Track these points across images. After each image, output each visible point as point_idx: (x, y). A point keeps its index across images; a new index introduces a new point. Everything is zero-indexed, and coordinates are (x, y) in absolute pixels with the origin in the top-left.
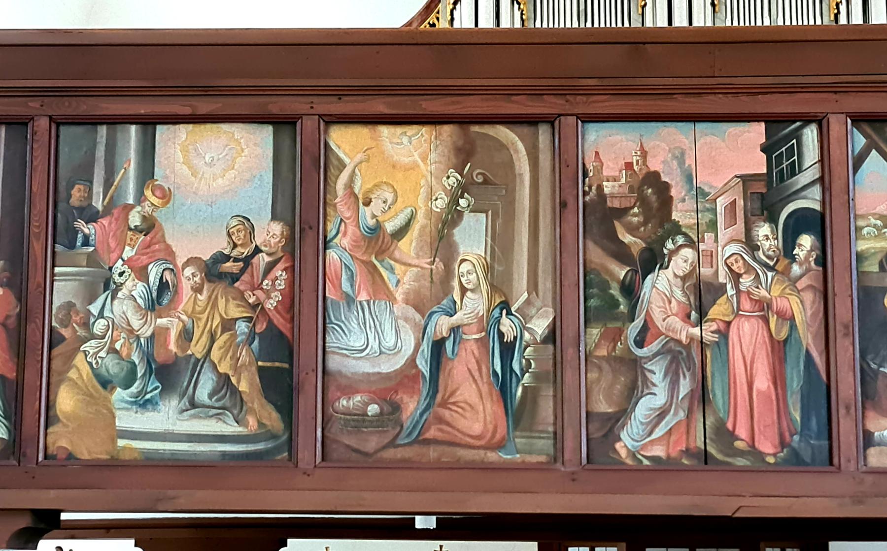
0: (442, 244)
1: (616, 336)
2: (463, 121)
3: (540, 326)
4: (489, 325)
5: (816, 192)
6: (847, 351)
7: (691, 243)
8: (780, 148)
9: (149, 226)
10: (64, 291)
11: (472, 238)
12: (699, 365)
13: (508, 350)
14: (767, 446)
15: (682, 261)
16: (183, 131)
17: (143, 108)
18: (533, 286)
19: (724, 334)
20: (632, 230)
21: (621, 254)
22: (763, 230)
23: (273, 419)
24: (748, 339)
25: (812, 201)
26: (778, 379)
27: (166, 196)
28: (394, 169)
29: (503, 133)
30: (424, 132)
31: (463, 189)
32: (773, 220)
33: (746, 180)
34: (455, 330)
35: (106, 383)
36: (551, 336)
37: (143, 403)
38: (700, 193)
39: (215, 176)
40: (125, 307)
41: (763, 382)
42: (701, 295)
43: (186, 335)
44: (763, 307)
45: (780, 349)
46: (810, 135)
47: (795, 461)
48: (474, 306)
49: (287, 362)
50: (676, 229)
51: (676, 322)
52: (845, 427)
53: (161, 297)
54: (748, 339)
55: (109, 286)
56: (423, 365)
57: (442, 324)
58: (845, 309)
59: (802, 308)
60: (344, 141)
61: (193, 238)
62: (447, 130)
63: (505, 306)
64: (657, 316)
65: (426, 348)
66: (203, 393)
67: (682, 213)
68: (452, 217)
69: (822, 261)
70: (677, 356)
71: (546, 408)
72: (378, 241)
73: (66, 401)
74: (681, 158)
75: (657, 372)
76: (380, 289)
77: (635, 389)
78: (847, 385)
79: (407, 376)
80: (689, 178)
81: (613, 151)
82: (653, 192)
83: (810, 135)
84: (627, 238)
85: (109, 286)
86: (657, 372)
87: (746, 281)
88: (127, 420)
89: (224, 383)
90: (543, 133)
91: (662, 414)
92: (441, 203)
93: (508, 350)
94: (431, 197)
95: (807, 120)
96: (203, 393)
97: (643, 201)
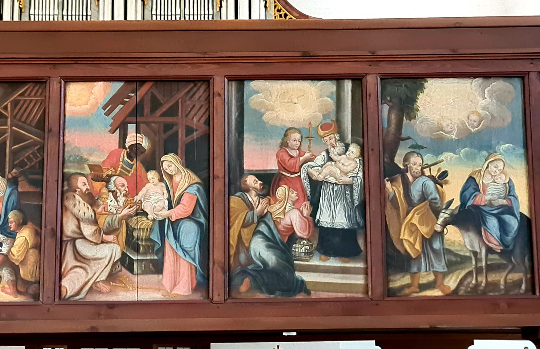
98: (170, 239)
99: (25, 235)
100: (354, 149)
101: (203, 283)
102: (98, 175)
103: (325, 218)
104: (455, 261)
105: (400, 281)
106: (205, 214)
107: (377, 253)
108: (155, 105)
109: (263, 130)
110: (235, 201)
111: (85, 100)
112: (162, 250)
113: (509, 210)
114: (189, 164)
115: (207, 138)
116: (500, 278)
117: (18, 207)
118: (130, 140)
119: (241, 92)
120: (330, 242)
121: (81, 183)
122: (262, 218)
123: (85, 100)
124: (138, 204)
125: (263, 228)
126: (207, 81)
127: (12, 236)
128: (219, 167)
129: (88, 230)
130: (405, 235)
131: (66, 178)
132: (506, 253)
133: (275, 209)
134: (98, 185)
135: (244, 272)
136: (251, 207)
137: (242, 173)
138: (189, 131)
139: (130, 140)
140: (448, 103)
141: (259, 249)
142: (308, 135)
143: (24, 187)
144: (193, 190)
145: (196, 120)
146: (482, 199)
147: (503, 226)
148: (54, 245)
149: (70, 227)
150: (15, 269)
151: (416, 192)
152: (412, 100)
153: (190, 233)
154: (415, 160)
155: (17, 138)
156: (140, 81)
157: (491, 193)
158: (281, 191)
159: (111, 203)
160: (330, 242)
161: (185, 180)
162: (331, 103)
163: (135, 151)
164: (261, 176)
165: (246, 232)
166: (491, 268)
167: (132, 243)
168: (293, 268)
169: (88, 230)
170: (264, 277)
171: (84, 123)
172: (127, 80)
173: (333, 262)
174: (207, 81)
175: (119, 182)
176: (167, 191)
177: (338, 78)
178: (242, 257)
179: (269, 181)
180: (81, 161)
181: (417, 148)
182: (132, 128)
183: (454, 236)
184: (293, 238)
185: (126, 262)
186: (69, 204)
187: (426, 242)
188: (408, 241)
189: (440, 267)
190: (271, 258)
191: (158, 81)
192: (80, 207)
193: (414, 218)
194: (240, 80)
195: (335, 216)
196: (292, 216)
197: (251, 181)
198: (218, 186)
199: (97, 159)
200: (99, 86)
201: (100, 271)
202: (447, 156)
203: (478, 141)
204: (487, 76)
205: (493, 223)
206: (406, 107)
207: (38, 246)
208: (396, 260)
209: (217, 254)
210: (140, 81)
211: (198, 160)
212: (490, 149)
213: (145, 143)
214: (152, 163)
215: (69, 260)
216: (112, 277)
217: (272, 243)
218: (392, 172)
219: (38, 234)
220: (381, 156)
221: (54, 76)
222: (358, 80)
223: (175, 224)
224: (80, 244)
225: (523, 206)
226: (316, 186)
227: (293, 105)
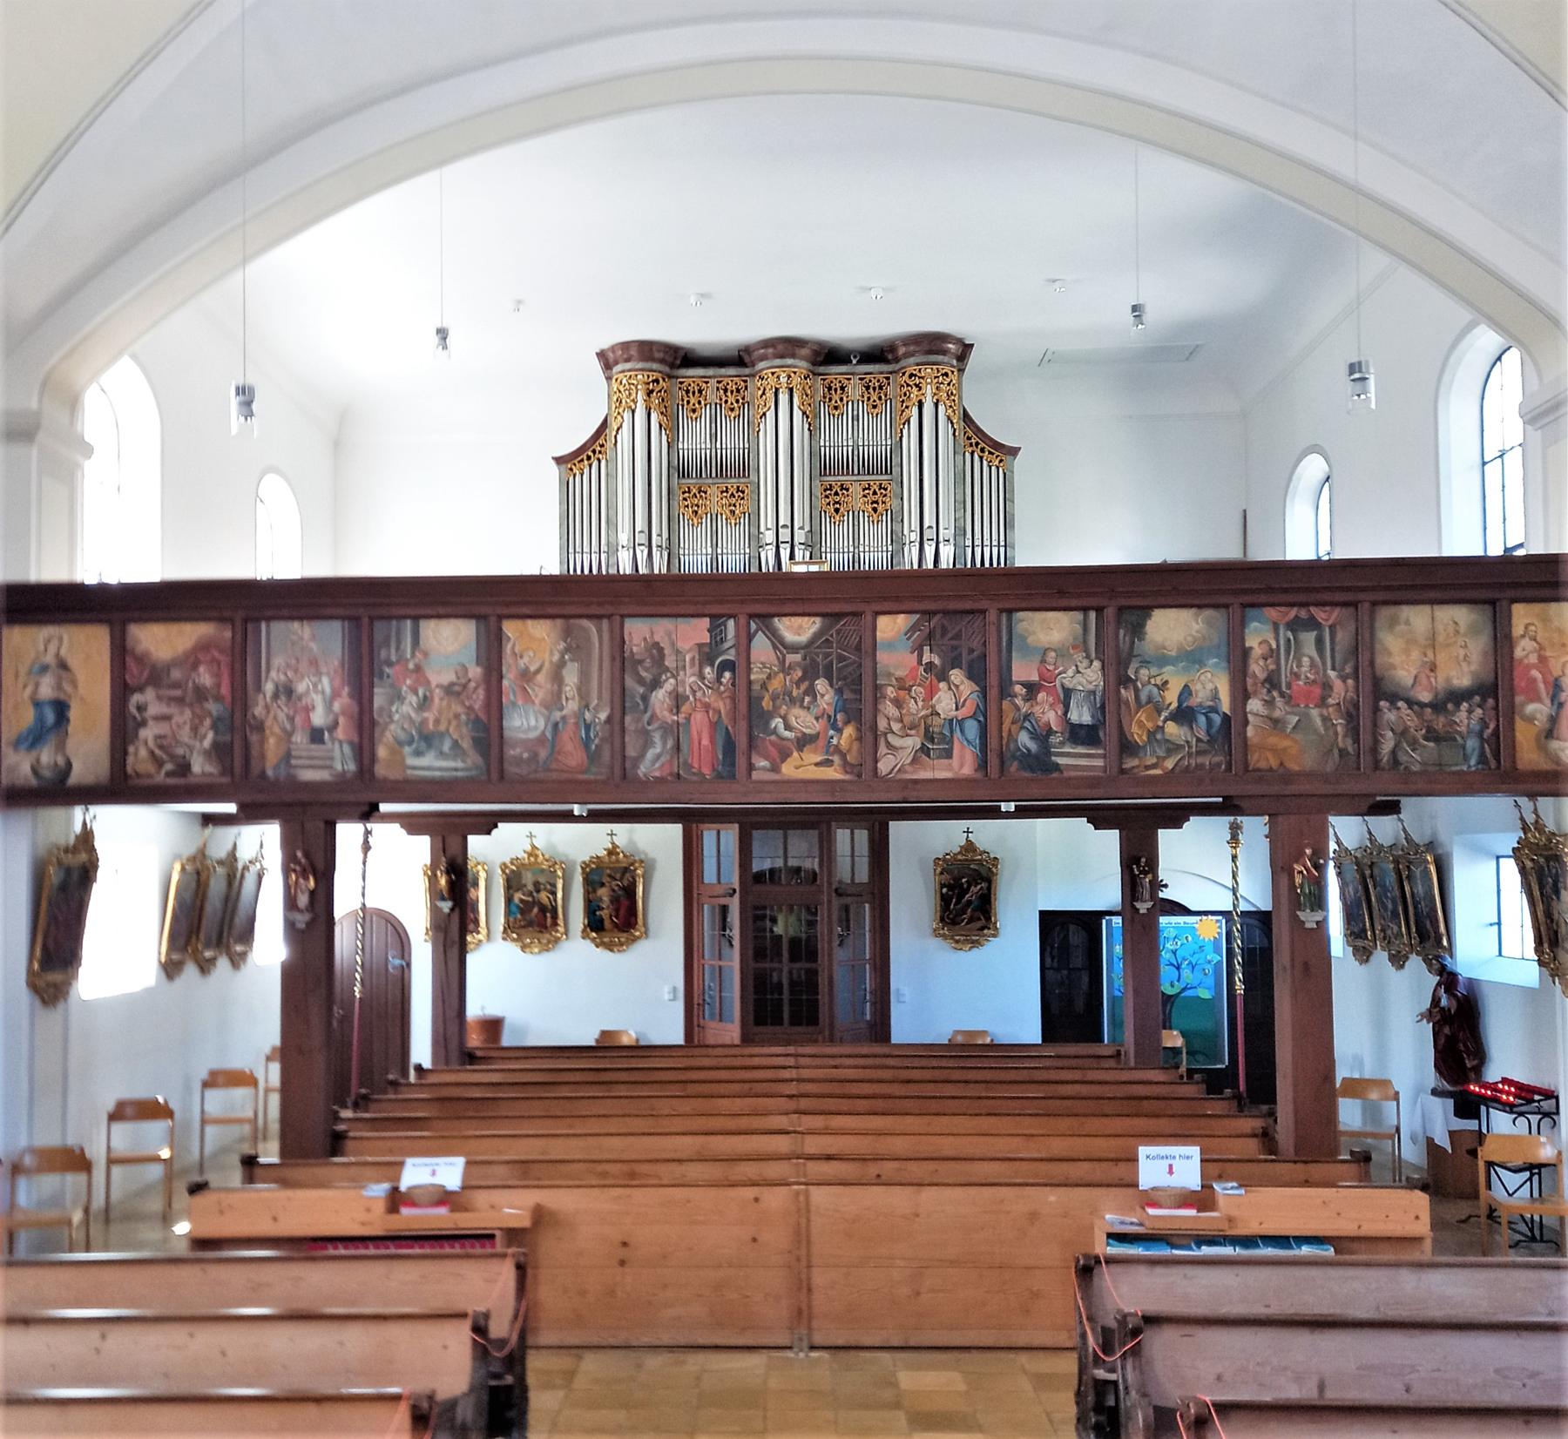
0: (557, 678)
1: (639, 720)
3: (603, 716)
4: (579, 715)
5: (733, 651)
7: (674, 676)
8: (716, 630)
11: (571, 677)
12: (675, 733)
13: (588, 728)
18: (600, 698)
19: (688, 719)
20: (647, 670)
21: (641, 681)
22: (708, 670)
24: (699, 719)
25: (730, 656)
26: (712, 741)
29: (585, 623)
31: (567, 650)
32: (712, 665)
33: (700, 646)
34: (564, 718)
36: (609, 720)
38: (678, 652)
41: (705, 742)
42: (678, 700)
44: (707, 706)
45: (714, 726)
46: (731, 623)
48: (572, 706)
50: (667, 669)
51: (666, 713)
56: (549, 735)
57: (557, 715)
58: (743, 707)
59: (723, 706)
62: (559, 622)
63: (587, 706)
64: (658, 711)
65: (550, 728)
67: (669, 662)
68: (561, 664)
69: (733, 685)
74: (669, 634)
77: (647, 744)
78: (742, 742)
80: (673, 644)
81: (638, 632)
84: (644, 674)
87: (699, 694)
90: (605, 623)
91: (658, 757)
92: (556, 657)
93: (588, 728)
94: (552, 654)
95: (730, 616)
97: (652, 657)
98: (958, 734)
99: (849, 731)
102: (903, 686)
106: (981, 715)
108: (944, 631)
109: (1027, 650)
110: (1006, 704)
112: (951, 742)
114: (971, 676)
117: (844, 710)
118: (925, 659)
119: (1010, 620)
121: (890, 692)
122: (1027, 717)
123: (891, 627)
124: (933, 707)
125: (1027, 724)
126: (983, 612)
127: (840, 731)
128: (993, 679)
129: (896, 727)
134: (902, 693)
135: (1014, 757)
136: (1018, 709)
138: (971, 651)
139: (925, 659)
143: (847, 695)
144: (974, 696)
145: (975, 643)
149: (882, 724)
153: (972, 728)
156: (935, 613)
161: (967, 688)
163: (930, 667)
165: (1014, 728)
167: (929, 736)
169: (896, 727)
171: (890, 645)
172: (923, 612)
174: (983, 612)
175: (918, 690)
176: (954, 697)
178: (1012, 746)
180: (889, 675)
182: (927, 649)
185: (924, 750)
186: (880, 707)
192: (890, 709)
194: (1010, 611)
197: (1018, 689)
198: (993, 693)
199: (900, 673)
207: (860, 739)
209: (993, 742)
210: (935, 613)
211: (977, 674)
213: (937, 661)
214: (943, 676)
216: (915, 761)
219: (859, 730)
221: (868, 609)
223: (961, 722)
224: (890, 737)
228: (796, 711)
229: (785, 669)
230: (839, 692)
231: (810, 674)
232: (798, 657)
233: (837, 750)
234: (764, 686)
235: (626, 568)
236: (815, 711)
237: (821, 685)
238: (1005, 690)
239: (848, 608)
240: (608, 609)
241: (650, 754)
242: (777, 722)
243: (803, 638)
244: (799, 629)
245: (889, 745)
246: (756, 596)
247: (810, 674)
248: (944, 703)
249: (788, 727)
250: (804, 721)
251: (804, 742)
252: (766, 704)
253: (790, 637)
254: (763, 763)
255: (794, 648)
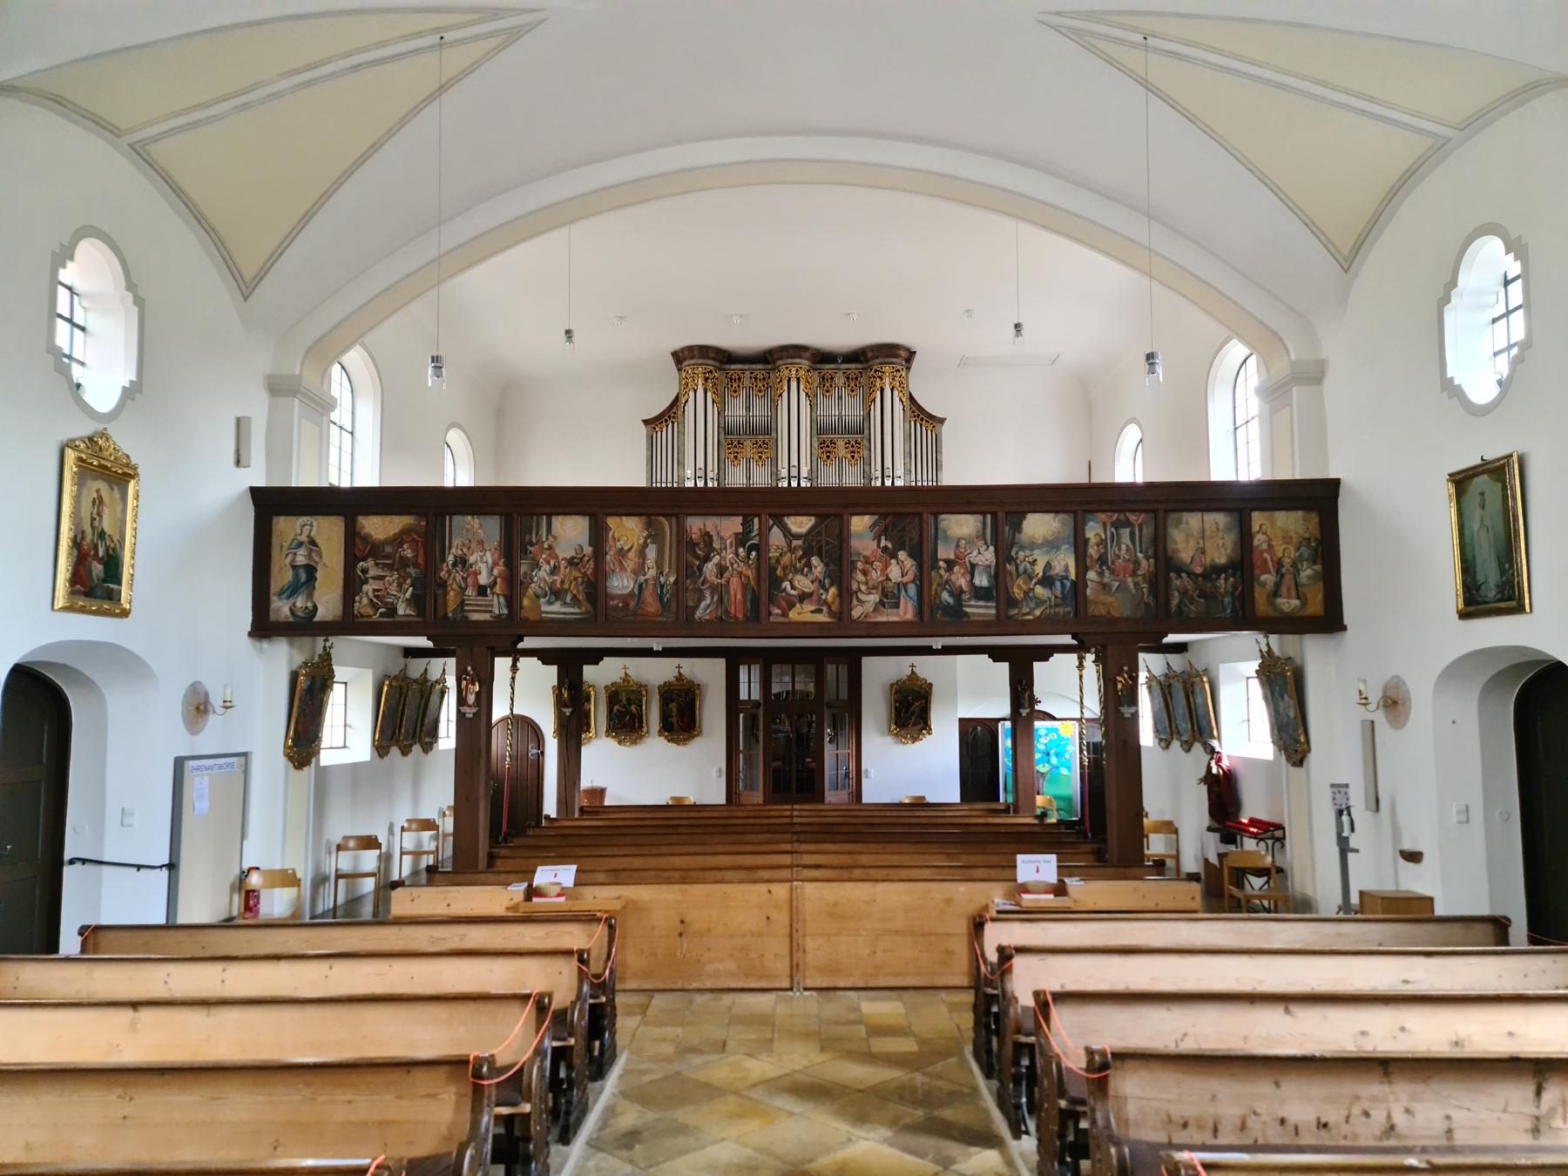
0: (642, 554)
1: (695, 583)
2: (649, 515)
3: (672, 579)
4: (656, 579)
6: (765, 586)
8: (747, 524)
9: (550, 547)
10: (523, 569)
11: (651, 553)
12: (720, 591)
13: (662, 587)
14: (740, 616)
15: (716, 559)
16: (560, 518)
17: (547, 510)
21: (697, 557)
23: (590, 608)
24: (735, 582)
25: (755, 541)
26: (744, 596)
27: (555, 538)
28: (627, 530)
29: (662, 519)
30: (637, 519)
33: (736, 534)
35: (538, 597)
36: (676, 582)
37: (550, 603)
39: (571, 532)
40: (543, 573)
41: (739, 597)
42: (721, 570)
43: (562, 582)
44: (740, 574)
45: (745, 587)
46: (756, 520)
47: (748, 620)
48: (652, 573)
49: (595, 587)
52: (763, 610)
53: (554, 570)
54: (735, 582)
55: (538, 567)
57: (642, 579)
58: (764, 574)
60: (612, 522)
61: (565, 552)
66: (568, 600)
67: (716, 545)
68: (645, 545)
70: (714, 589)
71: (674, 603)
72: (622, 553)
73: (526, 602)
75: (708, 594)
76: (623, 568)
77: (701, 598)
79: (632, 594)
81: (695, 525)
82: (707, 538)
83: (756, 520)
85: (538, 567)
86: (708, 594)
88: (544, 608)
89: (574, 597)
93: (662, 587)
96: (568, 600)
99: (833, 590)
100: (992, 548)
101: (920, 612)
102: (867, 561)
103: (977, 582)
104: (1040, 602)
105: (1014, 612)
106: (921, 579)
107: (1003, 598)
109: (946, 538)
111: (860, 524)
113: (1066, 578)
115: (921, 542)
116: (1061, 610)
120: (979, 593)
121: (860, 565)
122: (947, 582)
123: (860, 524)
127: (827, 591)
129: (863, 588)
130: (1016, 590)
131: (853, 562)
132: (1064, 598)
133: (953, 577)
137: (937, 560)
139: (883, 543)
140: (1038, 525)
141: (945, 596)
142: (969, 541)
145: (915, 534)
146: (1053, 573)
147: (1063, 585)
148: (847, 595)
149: (855, 586)
150: (829, 607)
151: (1021, 568)
152: (1020, 524)
153: (912, 589)
154: (1021, 554)
155: (828, 543)
157: (1058, 569)
158: (956, 569)
159: (874, 575)
160: (979, 593)
161: (909, 563)
162: (980, 525)
163: (885, 549)
164: (946, 561)
166: (1057, 605)
167: (885, 594)
168: (962, 606)
170: (946, 608)
171: (860, 535)
173: (981, 603)
174: (920, 515)
175: (877, 564)
176: (900, 569)
177: (984, 514)
179: (950, 564)
181: (1022, 548)
183: (1039, 590)
184: (961, 591)
185: (881, 603)
187: (1026, 593)
188: (1018, 593)
189: (1032, 605)
190: (951, 600)
191: (895, 514)
193: (1020, 582)
194: (936, 515)
195: (982, 580)
196: (962, 582)
199: (867, 553)
200: (867, 518)
201: (869, 608)
202: (1036, 552)
203: (1052, 544)
204: (1057, 512)
205: (1058, 584)
206: (1017, 527)
208: (1013, 603)
209: (926, 599)
211: (917, 554)
212: (1058, 548)
214: (894, 556)
215: (855, 602)
216: (875, 610)
217: (951, 594)
218: (1011, 560)
219: (840, 590)
220: (1005, 552)
222: (994, 515)
223: (905, 585)
225: (1073, 576)
226: (973, 566)
227: (962, 526)
228: (799, 577)
229: (792, 550)
230: (827, 565)
231: (808, 554)
232: (800, 542)
233: (825, 602)
234: (778, 561)
235: (690, 484)
236: (811, 577)
237: (815, 560)
238: (934, 566)
239: (830, 510)
240: (676, 510)
241: (703, 605)
242: (786, 584)
243: (804, 530)
244: (801, 524)
245: (859, 600)
246: (773, 503)
247: (808, 554)
248: (894, 572)
249: (793, 588)
250: (804, 583)
251: (803, 597)
252: (779, 572)
253: (794, 529)
254: (778, 611)
255: (797, 537)
